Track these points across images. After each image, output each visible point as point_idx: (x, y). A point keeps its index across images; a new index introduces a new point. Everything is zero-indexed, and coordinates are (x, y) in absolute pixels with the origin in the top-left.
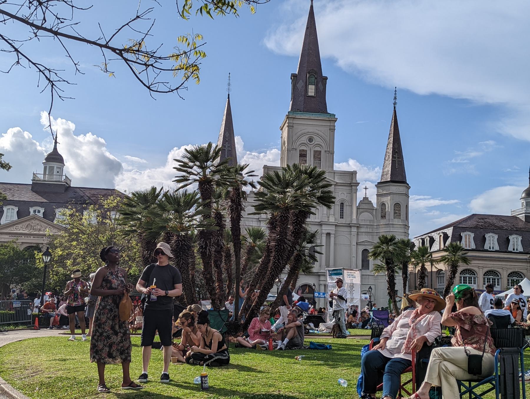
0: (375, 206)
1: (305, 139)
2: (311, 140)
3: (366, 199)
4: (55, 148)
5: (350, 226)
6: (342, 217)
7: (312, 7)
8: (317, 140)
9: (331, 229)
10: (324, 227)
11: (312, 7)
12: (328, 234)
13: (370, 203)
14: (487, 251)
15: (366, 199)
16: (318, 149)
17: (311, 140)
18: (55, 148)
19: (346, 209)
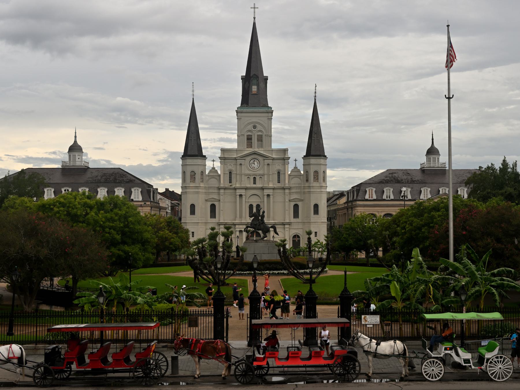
0: (302, 172)
1: (250, 127)
2: (255, 127)
3: (296, 168)
4: (75, 141)
5: (284, 189)
7: (254, 24)
8: (259, 127)
9: (270, 192)
10: (265, 191)
11: (254, 24)
12: (268, 196)
15: (296, 168)
16: (260, 133)
17: (255, 127)
18: (75, 141)
19: (282, 176)
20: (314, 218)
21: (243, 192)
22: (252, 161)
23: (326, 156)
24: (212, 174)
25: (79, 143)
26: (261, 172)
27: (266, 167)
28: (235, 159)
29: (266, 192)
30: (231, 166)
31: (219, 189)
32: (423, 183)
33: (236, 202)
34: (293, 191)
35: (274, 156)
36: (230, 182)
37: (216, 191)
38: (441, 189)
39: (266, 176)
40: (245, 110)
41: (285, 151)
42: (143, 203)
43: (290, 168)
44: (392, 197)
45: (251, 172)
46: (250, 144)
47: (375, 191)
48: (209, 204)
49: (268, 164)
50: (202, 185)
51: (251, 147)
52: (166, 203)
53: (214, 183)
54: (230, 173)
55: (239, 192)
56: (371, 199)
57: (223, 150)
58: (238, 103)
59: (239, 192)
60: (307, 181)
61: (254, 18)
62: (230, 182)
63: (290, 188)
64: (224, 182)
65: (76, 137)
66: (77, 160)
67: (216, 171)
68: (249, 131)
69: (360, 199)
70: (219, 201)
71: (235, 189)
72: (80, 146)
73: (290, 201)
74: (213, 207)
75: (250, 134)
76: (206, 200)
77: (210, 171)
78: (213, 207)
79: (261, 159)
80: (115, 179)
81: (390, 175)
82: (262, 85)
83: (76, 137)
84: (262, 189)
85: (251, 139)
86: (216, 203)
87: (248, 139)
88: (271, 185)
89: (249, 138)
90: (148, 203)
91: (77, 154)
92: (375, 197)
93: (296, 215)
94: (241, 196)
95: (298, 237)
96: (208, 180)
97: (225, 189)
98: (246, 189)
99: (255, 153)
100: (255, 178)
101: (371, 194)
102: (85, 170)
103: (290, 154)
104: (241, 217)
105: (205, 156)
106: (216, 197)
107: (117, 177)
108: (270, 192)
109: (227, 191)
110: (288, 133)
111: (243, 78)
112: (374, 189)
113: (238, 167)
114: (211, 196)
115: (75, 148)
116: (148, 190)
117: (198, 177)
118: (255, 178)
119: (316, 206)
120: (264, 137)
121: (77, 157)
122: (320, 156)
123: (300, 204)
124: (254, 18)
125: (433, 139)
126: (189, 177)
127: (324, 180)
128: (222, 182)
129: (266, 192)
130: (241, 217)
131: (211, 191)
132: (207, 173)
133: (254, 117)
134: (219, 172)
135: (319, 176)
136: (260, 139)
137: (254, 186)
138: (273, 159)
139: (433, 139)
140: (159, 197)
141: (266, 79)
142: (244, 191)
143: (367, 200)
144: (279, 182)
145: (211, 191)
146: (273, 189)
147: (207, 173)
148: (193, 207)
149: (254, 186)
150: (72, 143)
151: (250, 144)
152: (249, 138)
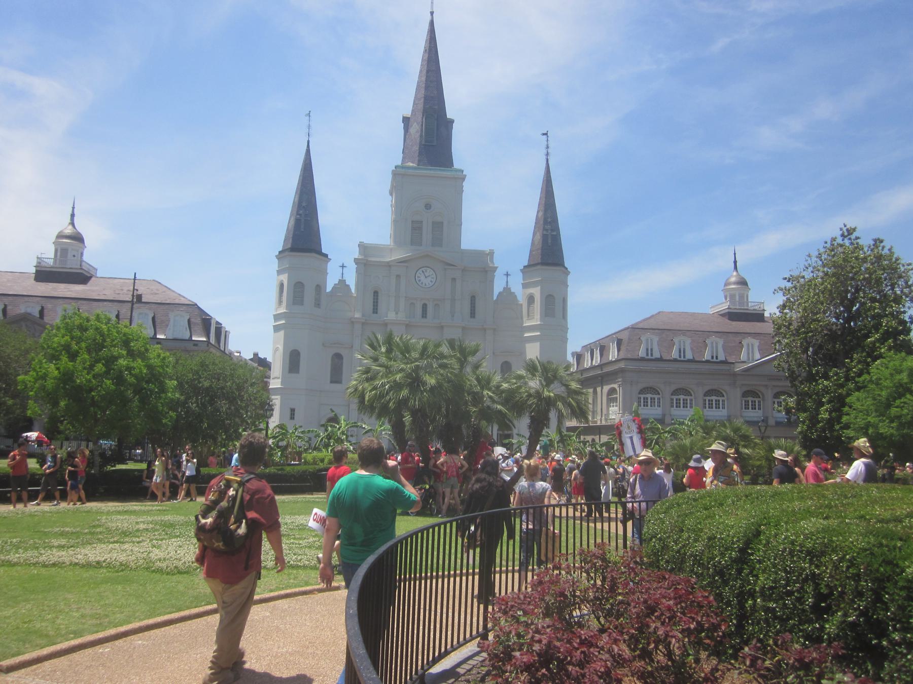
2: (428, 206)
7: (432, 23)
11: (432, 23)
17: (428, 206)
22: (420, 271)
28: (389, 265)
54: (376, 293)
56: (650, 357)
57: (363, 247)
61: (432, 13)
85: (420, 229)
89: (417, 227)
100: (425, 307)
103: (497, 261)
105: (326, 256)
111: (406, 120)
117: (309, 295)
118: (425, 307)
124: (432, 13)
127: (564, 316)
132: (329, 289)
135: (555, 307)
136: (438, 226)
138: (464, 270)
141: (452, 122)
147: (329, 289)
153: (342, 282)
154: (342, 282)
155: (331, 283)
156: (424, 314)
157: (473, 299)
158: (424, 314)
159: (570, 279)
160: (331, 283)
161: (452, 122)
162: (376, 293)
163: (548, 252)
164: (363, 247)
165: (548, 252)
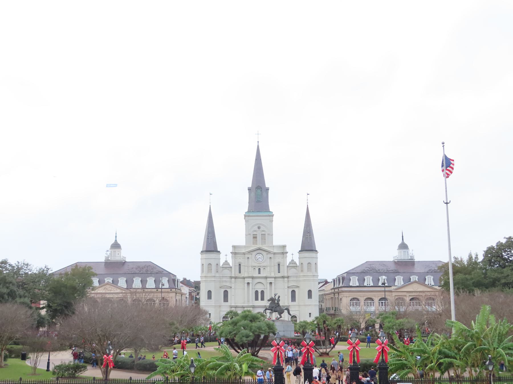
0: (298, 264)
1: (256, 228)
2: (259, 228)
4: (116, 240)
5: (283, 277)
6: (279, 272)
7: (258, 147)
8: (262, 228)
9: (272, 280)
10: (268, 279)
11: (258, 147)
12: (271, 283)
13: (295, 263)
14: (366, 286)
16: (263, 233)
17: (259, 228)
18: (116, 240)
20: (308, 301)
21: (250, 280)
23: (316, 251)
24: (225, 266)
25: (119, 242)
26: (265, 264)
27: (269, 260)
28: (244, 254)
29: (269, 280)
30: (240, 259)
31: (231, 277)
32: (397, 273)
33: (244, 289)
34: (290, 279)
35: (275, 251)
36: (240, 272)
37: (229, 280)
38: (411, 277)
39: (269, 267)
40: (251, 214)
41: (284, 247)
42: (169, 290)
43: (289, 260)
44: (372, 284)
45: (256, 264)
46: (255, 243)
47: (358, 280)
48: (222, 290)
49: (270, 258)
50: (217, 275)
51: (257, 244)
52: (186, 290)
53: (227, 273)
54: (240, 265)
55: (247, 280)
57: (234, 247)
58: (245, 208)
59: (247, 280)
60: (302, 271)
62: (240, 272)
63: (288, 277)
64: (235, 272)
65: (116, 237)
66: (117, 255)
67: (229, 264)
68: (255, 231)
69: (345, 286)
70: (231, 287)
71: (244, 278)
72: (119, 244)
73: (288, 287)
74: (226, 293)
75: (255, 233)
76: (220, 287)
77: (224, 264)
78: (226, 293)
79: (264, 253)
80: (147, 271)
81: (369, 266)
82: (264, 194)
83: (116, 237)
84: (266, 278)
86: (228, 290)
87: (254, 238)
88: (273, 275)
89: (255, 237)
90: (174, 290)
91: (117, 250)
92: (357, 284)
93: (293, 298)
94: (248, 283)
95: (295, 317)
96: (222, 270)
97: (236, 278)
98: (253, 278)
99: (259, 249)
100: (259, 269)
101: (354, 281)
102: (123, 263)
103: (288, 249)
104: (248, 301)
105: (219, 252)
106: (228, 284)
107: (148, 270)
108: (272, 280)
109: (237, 280)
110: (286, 232)
111: (249, 189)
112: (357, 278)
113: (246, 260)
114: (225, 284)
115: (116, 246)
116: (173, 280)
117: (214, 267)
118: (259, 269)
119: (310, 292)
120: (266, 235)
121: (117, 253)
122: (312, 250)
123: (296, 290)
125: (403, 237)
126: (207, 268)
128: (233, 273)
129: (269, 280)
130: (248, 301)
131: (224, 279)
132: (221, 265)
133: (259, 220)
134: (231, 265)
135: (312, 267)
137: (259, 275)
139: (403, 237)
140: (181, 285)
141: (268, 189)
142: (251, 279)
143: (351, 287)
144: (279, 272)
145: (224, 279)
146: (275, 278)
147: (221, 265)
148: (209, 292)
149: (259, 275)
150: (113, 241)
151: (255, 243)
152: (255, 237)
153: (226, 261)
154: (226, 261)
155: (222, 262)
156: (259, 273)
157: (279, 265)
158: (259, 273)
159: (319, 255)
160: (222, 262)
161: (268, 189)
162: (240, 265)
163: (308, 246)
164: (234, 247)
165: (308, 246)
